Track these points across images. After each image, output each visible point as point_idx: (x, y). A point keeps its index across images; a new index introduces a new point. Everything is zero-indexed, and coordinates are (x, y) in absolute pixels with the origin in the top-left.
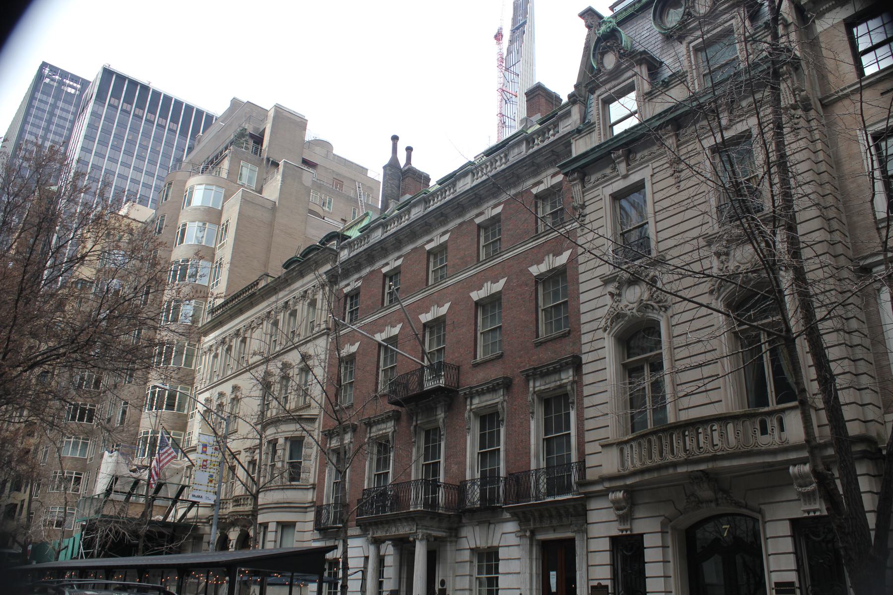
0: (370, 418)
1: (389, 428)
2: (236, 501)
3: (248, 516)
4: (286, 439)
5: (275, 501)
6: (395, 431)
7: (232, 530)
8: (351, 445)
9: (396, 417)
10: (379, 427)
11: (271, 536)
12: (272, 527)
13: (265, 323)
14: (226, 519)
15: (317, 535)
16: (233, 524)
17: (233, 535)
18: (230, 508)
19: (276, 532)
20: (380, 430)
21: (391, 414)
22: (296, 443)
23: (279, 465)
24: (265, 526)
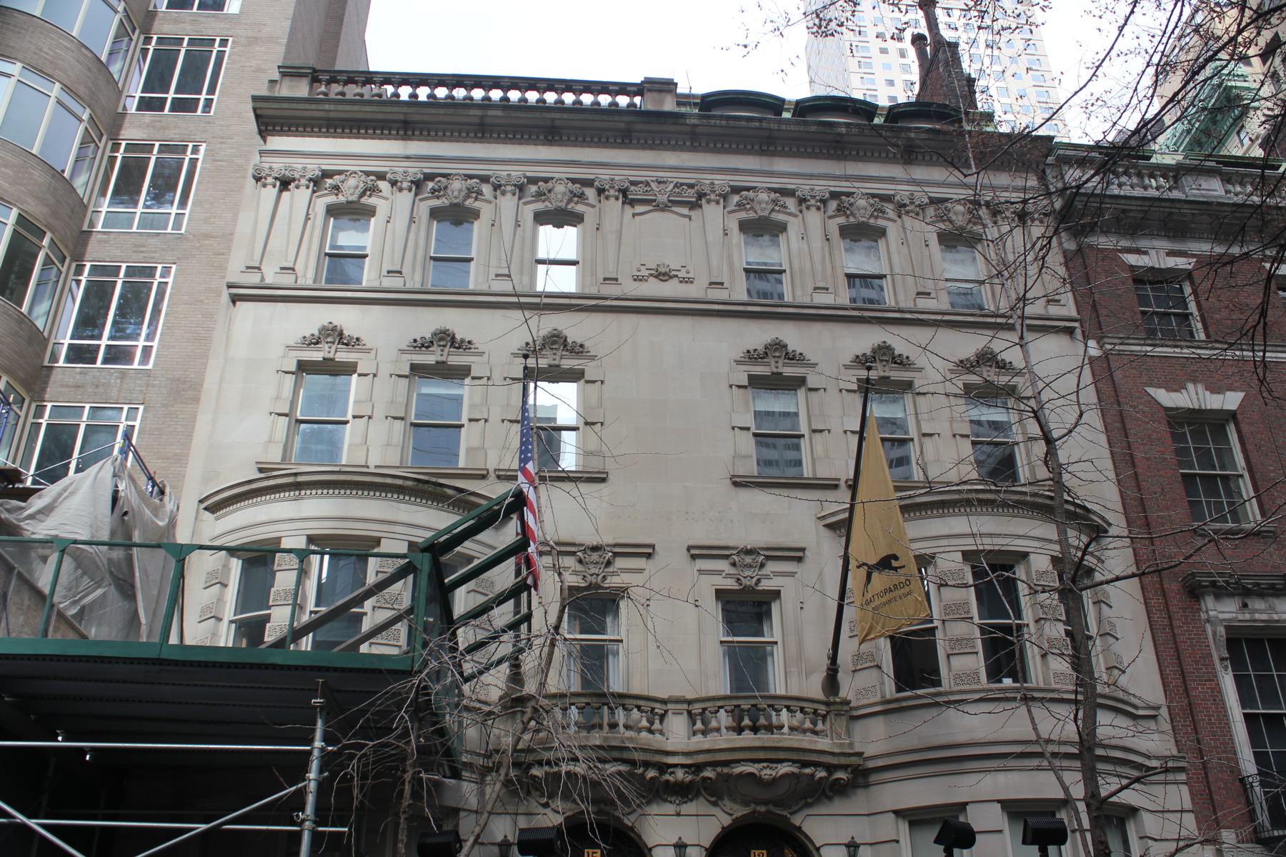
3: (830, 768)
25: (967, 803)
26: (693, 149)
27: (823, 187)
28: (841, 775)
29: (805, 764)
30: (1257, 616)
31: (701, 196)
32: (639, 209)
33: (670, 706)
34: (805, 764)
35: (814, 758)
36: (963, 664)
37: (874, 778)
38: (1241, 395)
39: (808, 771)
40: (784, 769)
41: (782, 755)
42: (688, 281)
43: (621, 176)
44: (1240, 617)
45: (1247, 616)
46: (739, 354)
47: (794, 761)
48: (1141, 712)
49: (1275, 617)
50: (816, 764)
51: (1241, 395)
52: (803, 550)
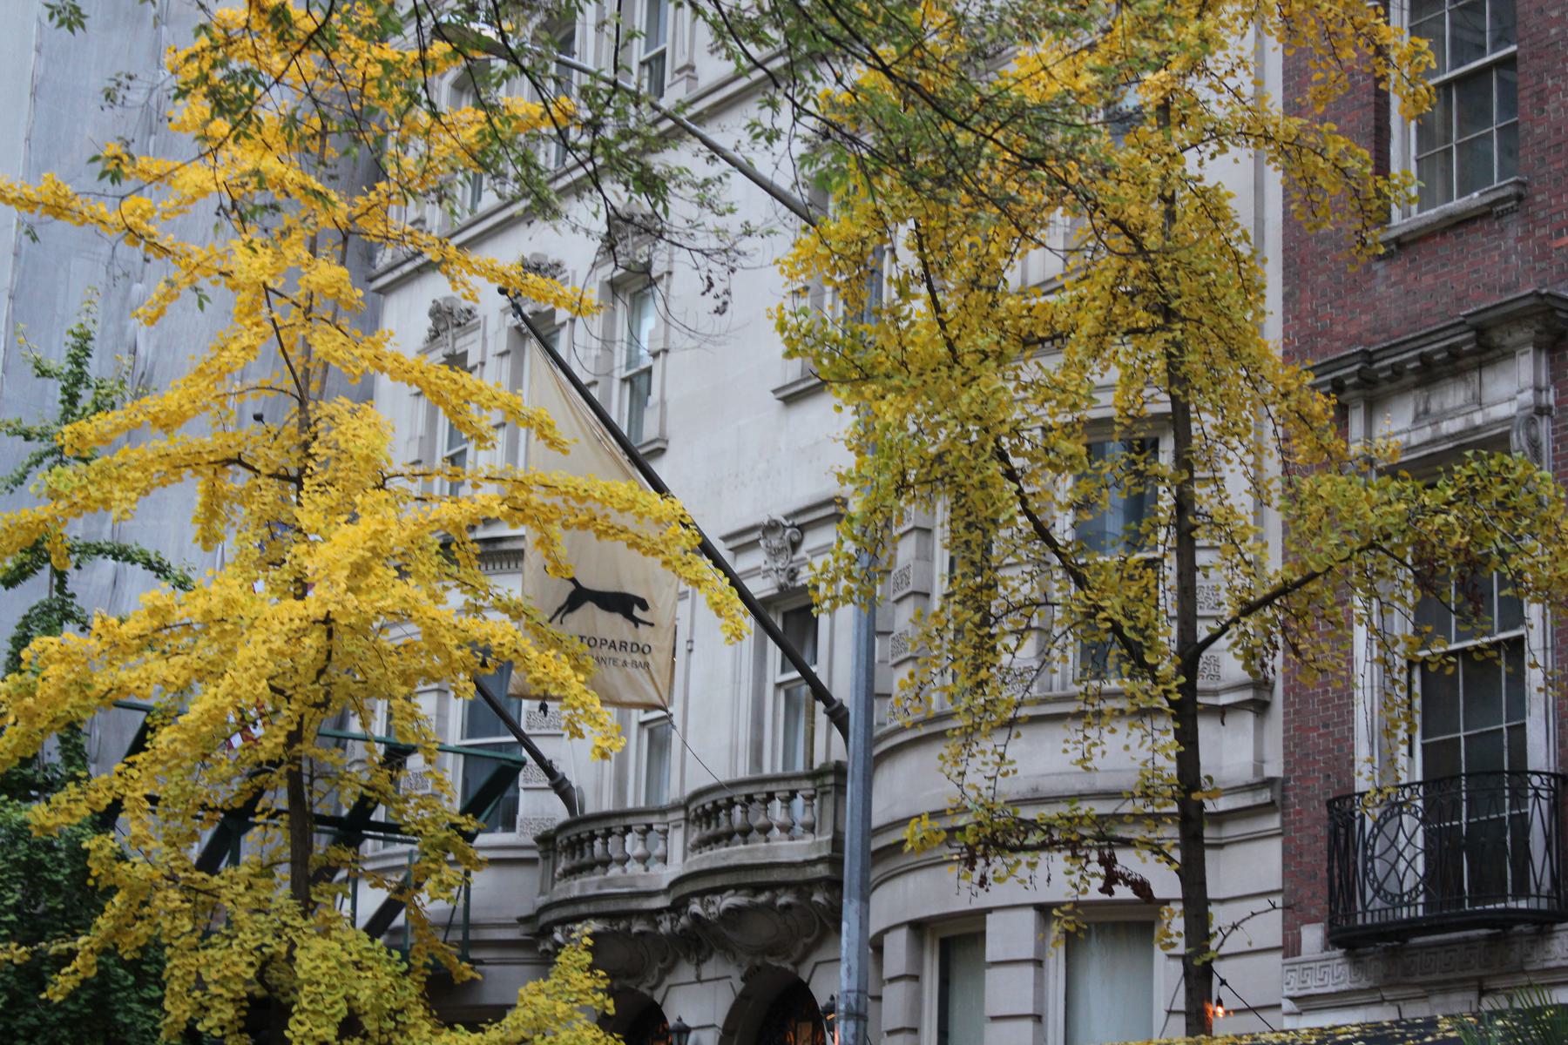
2: (708, 816)
7: (686, 971)
8: (1544, 427)
12: (1009, 935)
14: (652, 915)
15: (1337, 975)
16: (698, 942)
17: (699, 1004)
18: (676, 857)
19: (1038, 963)
23: (903, 617)
25: (990, 910)
28: (818, 898)
29: (757, 889)
30: (1449, 427)
33: (671, 817)
34: (757, 889)
35: (776, 876)
39: (763, 898)
40: (729, 901)
41: (719, 881)
44: (1415, 439)
45: (1427, 433)
47: (737, 888)
48: (1224, 700)
49: (1478, 419)
50: (773, 887)
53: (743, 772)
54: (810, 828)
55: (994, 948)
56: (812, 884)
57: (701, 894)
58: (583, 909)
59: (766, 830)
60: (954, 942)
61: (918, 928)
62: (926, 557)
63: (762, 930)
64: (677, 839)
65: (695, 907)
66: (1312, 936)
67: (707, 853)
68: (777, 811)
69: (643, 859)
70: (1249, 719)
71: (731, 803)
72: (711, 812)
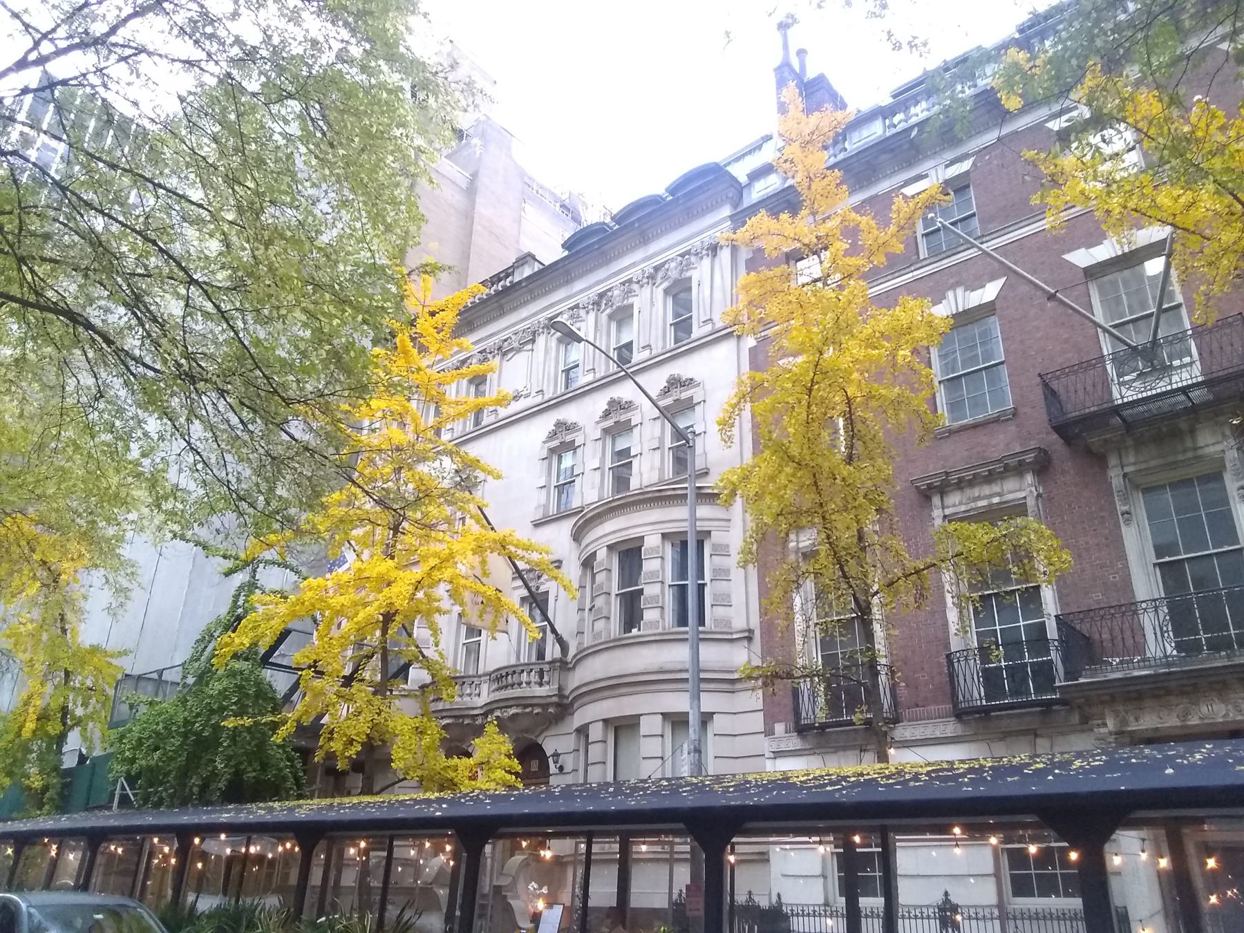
0: (947, 474)
1: (1023, 489)
2: (498, 679)
3: (545, 706)
4: (664, 536)
5: (655, 667)
6: (1039, 496)
9: (1042, 466)
10: (976, 492)
11: (650, 747)
12: (651, 725)
13: (541, 340)
14: (474, 717)
15: (795, 742)
18: (485, 695)
20: (979, 498)
21: (1029, 458)
22: (688, 548)
24: (624, 727)
26: (534, 299)
27: (593, 294)
28: (551, 710)
31: (534, 333)
32: (510, 356)
36: (658, 614)
37: (575, 706)
38: (1067, 257)
39: (528, 710)
42: (527, 396)
43: (496, 340)
46: (544, 436)
47: (517, 706)
48: (735, 636)
50: (532, 705)
51: (1067, 257)
52: (560, 562)
53: (513, 661)
54: (548, 683)
55: (644, 730)
56: (549, 705)
57: (501, 708)
58: (444, 714)
59: (520, 684)
60: (624, 727)
61: (606, 721)
62: (609, 579)
63: (525, 723)
64: (485, 688)
65: (498, 713)
66: (779, 728)
67: (503, 692)
68: (524, 677)
69: (470, 695)
70: (745, 643)
71: (507, 674)
72: (501, 677)
